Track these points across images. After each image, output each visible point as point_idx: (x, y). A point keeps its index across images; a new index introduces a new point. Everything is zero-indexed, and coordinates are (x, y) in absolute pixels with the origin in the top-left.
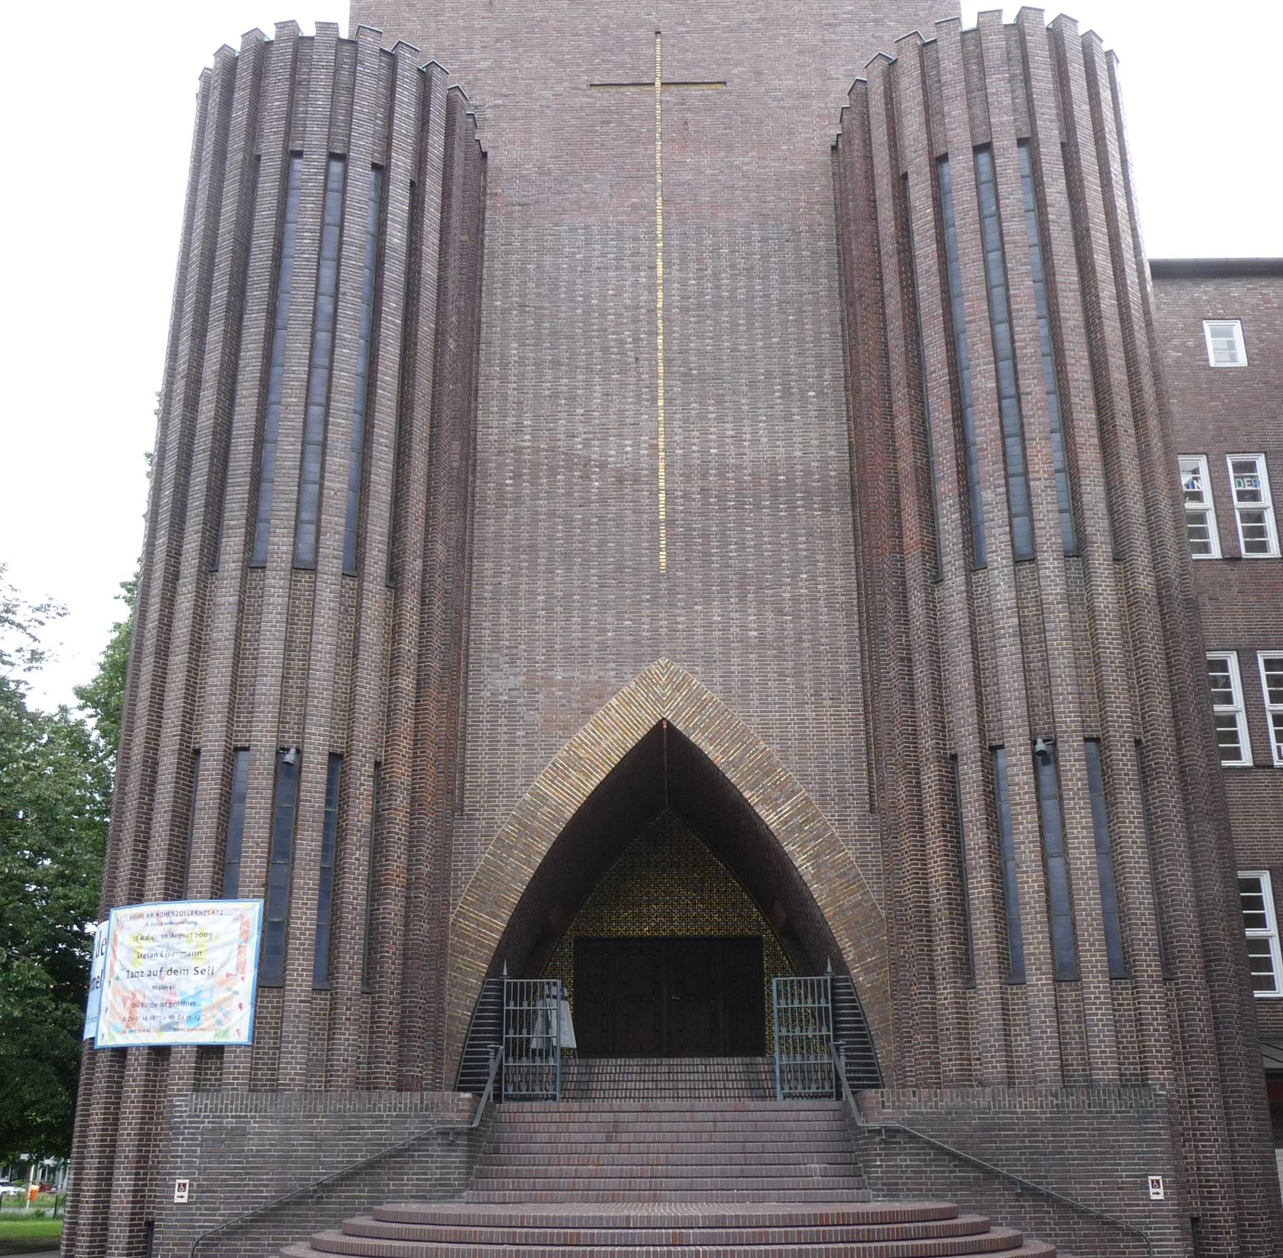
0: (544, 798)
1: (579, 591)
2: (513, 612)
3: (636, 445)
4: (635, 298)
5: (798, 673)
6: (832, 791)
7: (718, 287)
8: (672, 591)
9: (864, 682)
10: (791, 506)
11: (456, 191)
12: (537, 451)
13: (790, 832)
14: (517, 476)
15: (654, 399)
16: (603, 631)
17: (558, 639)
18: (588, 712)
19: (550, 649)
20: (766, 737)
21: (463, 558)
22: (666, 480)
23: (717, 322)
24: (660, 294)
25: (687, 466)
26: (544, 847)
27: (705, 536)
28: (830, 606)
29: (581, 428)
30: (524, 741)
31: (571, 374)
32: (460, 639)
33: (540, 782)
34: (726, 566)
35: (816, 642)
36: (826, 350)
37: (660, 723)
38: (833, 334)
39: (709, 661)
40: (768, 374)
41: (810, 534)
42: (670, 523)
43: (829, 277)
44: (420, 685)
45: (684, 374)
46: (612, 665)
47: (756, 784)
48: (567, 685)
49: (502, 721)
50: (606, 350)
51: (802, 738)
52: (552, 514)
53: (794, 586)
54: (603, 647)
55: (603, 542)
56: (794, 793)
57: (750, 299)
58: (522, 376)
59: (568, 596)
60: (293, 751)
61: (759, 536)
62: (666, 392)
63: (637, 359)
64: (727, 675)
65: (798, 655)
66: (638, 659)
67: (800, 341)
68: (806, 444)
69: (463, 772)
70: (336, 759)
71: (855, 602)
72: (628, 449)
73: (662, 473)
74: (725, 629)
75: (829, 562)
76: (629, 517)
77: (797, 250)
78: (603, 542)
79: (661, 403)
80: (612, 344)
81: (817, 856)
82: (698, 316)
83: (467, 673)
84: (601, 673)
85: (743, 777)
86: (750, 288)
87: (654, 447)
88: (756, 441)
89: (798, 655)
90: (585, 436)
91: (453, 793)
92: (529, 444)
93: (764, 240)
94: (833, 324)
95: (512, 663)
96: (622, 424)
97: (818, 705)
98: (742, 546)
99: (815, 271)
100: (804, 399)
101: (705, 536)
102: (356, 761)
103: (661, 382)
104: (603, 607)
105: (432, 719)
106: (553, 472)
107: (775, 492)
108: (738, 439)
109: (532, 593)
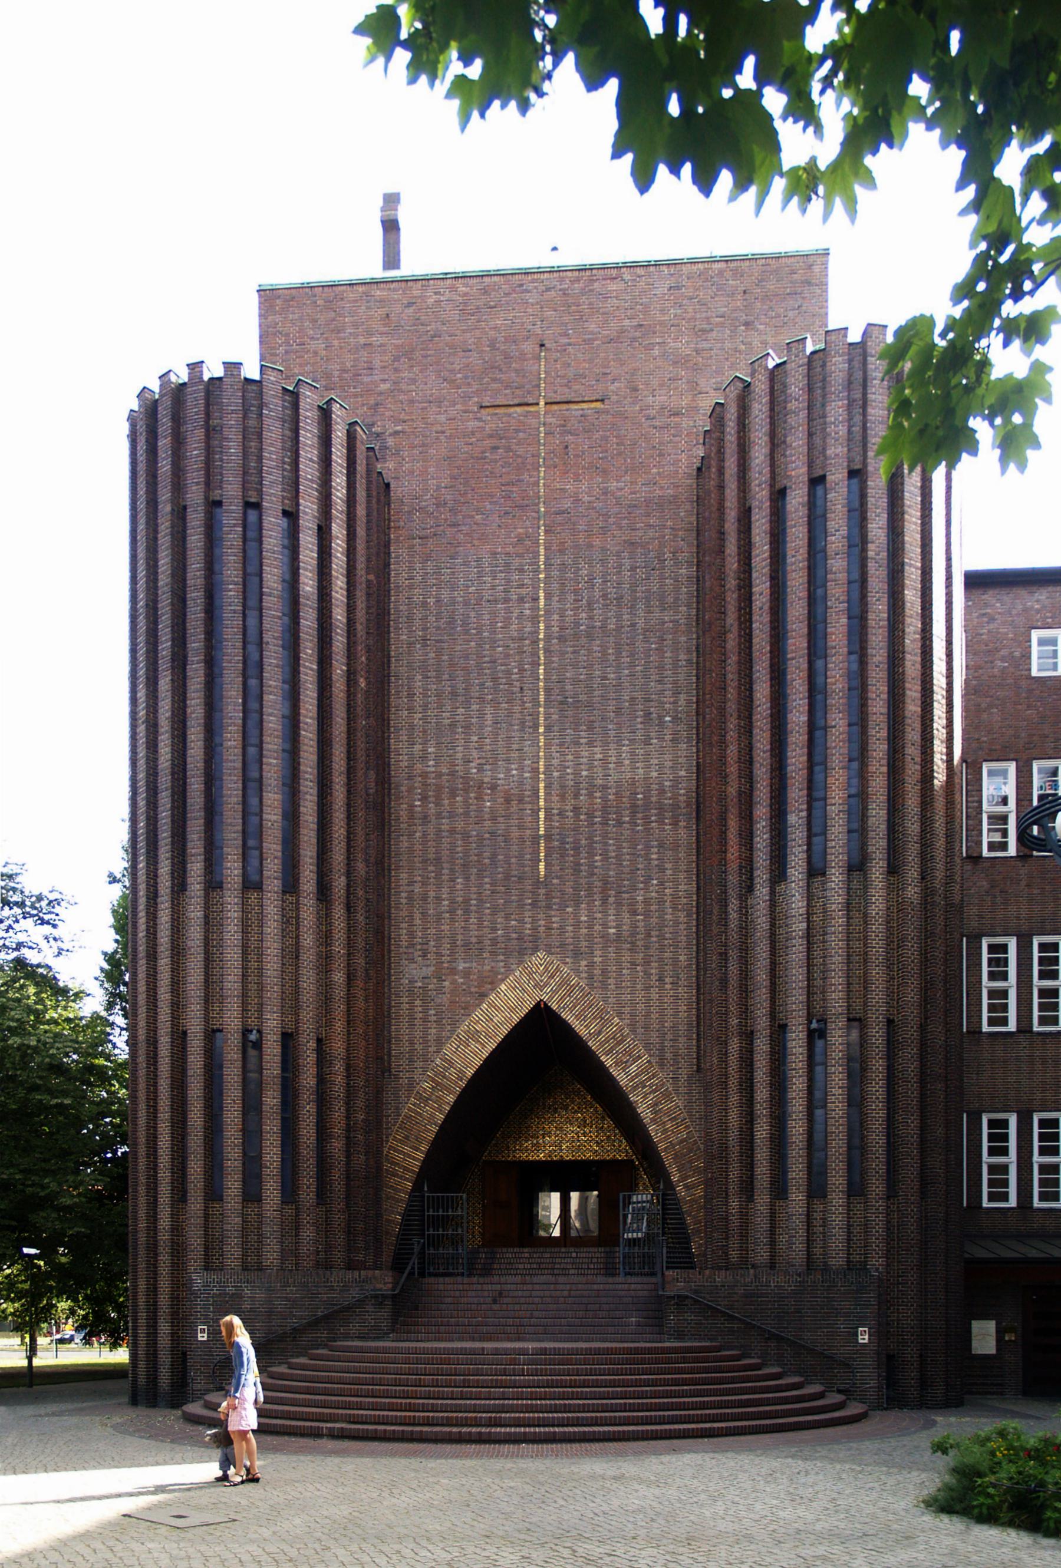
0: (451, 1063)
1: (475, 896)
2: (424, 914)
3: (521, 769)
4: (520, 630)
5: (647, 963)
6: (668, 1056)
7: (591, 618)
8: (548, 896)
9: (698, 969)
10: (647, 822)
11: (361, 532)
12: (440, 775)
13: (635, 1088)
14: (424, 798)
15: (536, 726)
16: (494, 929)
17: (460, 937)
18: (483, 996)
19: (454, 944)
20: (620, 1014)
21: (383, 870)
22: (546, 800)
23: (590, 651)
24: (542, 626)
25: (563, 787)
26: (451, 1099)
27: (576, 849)
28: (674, 908)
29: (475, 754)
30: (435, 1018)
31: (467, 704)
32: (383, 938)
33: (447, 1050)
34: (593, 874)
35: (661, 937)
36: (682, 677)
37: (538, 1004)
38: (689, 661)
39: (577, 954)
40: (633, 699)
41: (661, 846)
42: (548, 837)
43: (689, 606)
44: (350, 978)
45: (561, 703)
46: (502, 957)
47: (610, 1051)
48: (467, 973)
49: (418, 1002)
50: (495, 679)
51: (648, 1014)
52: (452, 831)
53: (646, 889)
54: (494, 942)
55: (493, 857)
56: (639, 1057)
57: (619, 628)
58: (425, 707)
59: (467, 901)
60: (255, 1032)
61: (619, 848)
62: (546, 719)
63: (522, 688)
64: (591, 965)
65: (647, 948)
66: (522, 952)
67: (661, 668)
68: (661, 766)
69: (389, 1042)
70: (288, 1039)
71: (694, 903)
72: (514, 772)
73: (542, 793)
74: (590, 927)
75: (675, 870)
76: (515, 834)
77: (662, 577)
78: (493, 857)
79: (541, 730)
80: (500, 675)
81: (656, 1104)
82: (574, 646)
83: (389, 964)
84: (493, 964)
85: (601, 1045)
86: (619, 617)
87: (535, 771)
88: (619, 763)
89: (647, 948)
90: (478, 761)
91: (382, 1059)
92: (433, 769)
93: (633, 569)
94: (689, 652)
95: (424, 956)
96: (509, 750)
97: (661, 988)
98: (605, 857)
99: (677, 599)
100: (661, 723)
101: (576, 849)
102: (302, 1039)
103: (541, 709)
104: (495, 910)
105: (361, 1004)
106: (453, 794)
107: (634, 809)
108: (605, 761)
109: (438, 899)
